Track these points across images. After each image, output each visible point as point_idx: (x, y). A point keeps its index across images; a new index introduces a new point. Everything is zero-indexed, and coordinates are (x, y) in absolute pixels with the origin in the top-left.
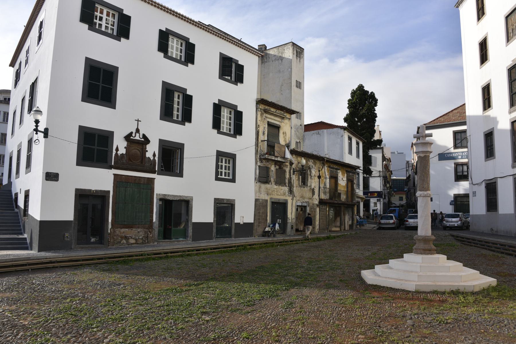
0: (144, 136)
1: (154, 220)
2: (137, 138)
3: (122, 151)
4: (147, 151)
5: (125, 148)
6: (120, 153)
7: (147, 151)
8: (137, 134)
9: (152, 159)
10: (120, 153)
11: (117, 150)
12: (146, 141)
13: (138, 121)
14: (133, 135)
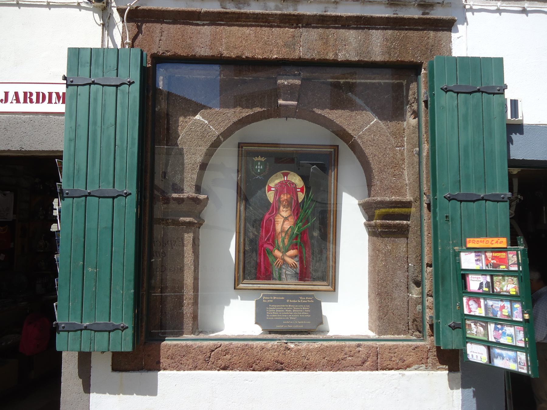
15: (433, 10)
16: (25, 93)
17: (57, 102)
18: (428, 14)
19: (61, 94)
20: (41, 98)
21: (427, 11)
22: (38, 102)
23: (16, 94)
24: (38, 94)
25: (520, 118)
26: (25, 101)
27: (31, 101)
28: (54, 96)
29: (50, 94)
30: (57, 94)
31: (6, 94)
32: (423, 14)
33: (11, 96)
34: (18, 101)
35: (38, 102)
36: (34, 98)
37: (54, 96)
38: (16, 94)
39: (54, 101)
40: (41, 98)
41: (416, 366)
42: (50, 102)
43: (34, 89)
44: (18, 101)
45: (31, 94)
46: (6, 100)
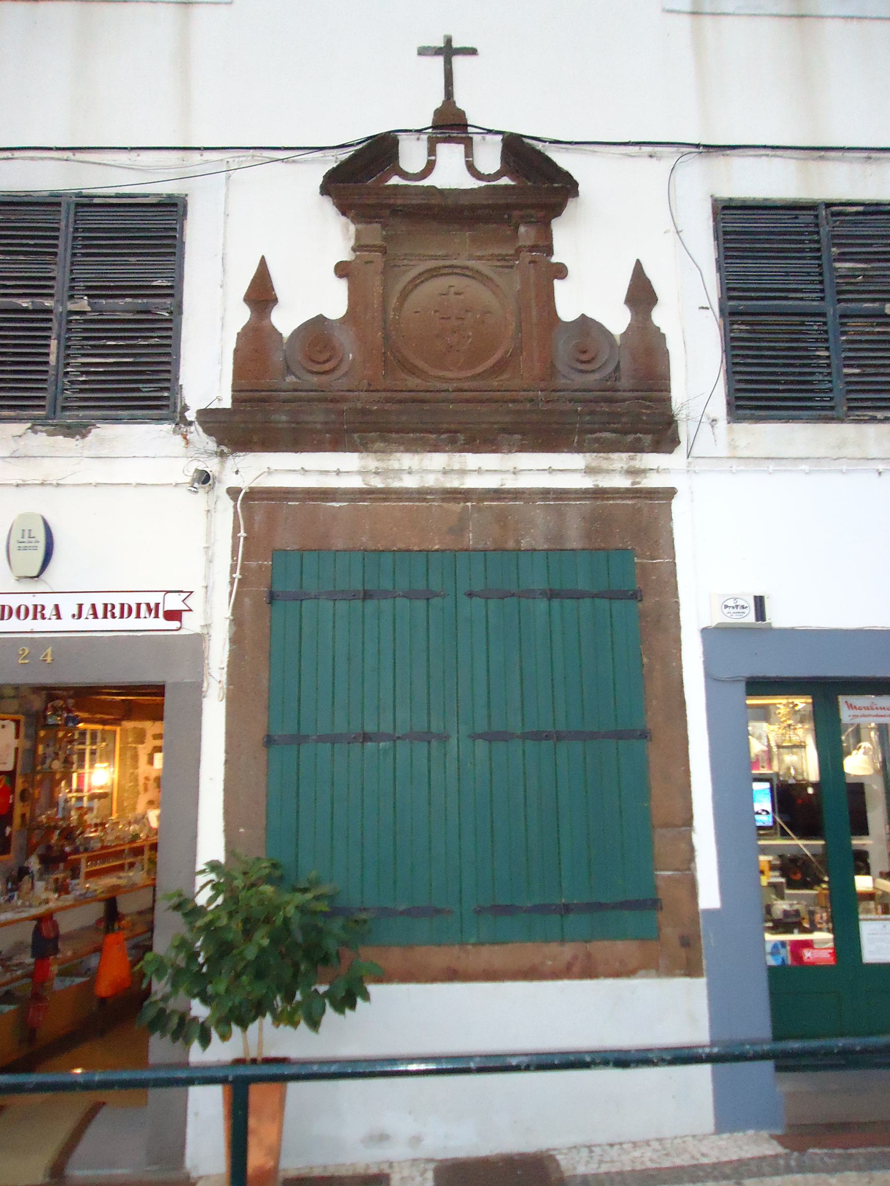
0: (519, 152)
1: (709, 896)
2: (451, 172)
3: (312, 293)
4: (561, 271)
5: (342, 270)
6: (286, 320)
7: (561, 271)
8: (450, 156)
9: (617, 320)
10: (286, 320)
11: (261, 294)
12: (536, 183)
13: (448, 51)
14: (412, 156)
15: (645, 477)
16: (106, 605)
17: (147, 615)
18: (639, 483)
19: (153, 606)
20: (125, 611)
21: (638, 480)
22: (122, 616)
23: (93, 606)
24: (122, 605)
25: (768, 621)
26: (105, 617)
27: (113, 616)
28: (143, 608)
29: (139, 605)
30: (148, 605)
31: (80, 606)
32: (633, 484)
33: (86, 610)
34: (95, 616)
35: (122, 616)
36: (117, 611)
37: (143, 608)
38: (93, 606)
39: (142, 615)
40: (125, 611)
41: (642, 972)
42: (138, 616)
43: (116, 600)
44: (95, 616)
45: (113, 607)
46: (80, 616)
